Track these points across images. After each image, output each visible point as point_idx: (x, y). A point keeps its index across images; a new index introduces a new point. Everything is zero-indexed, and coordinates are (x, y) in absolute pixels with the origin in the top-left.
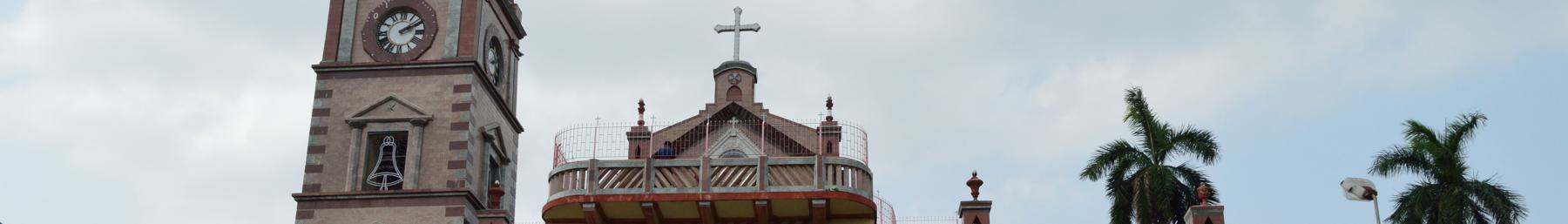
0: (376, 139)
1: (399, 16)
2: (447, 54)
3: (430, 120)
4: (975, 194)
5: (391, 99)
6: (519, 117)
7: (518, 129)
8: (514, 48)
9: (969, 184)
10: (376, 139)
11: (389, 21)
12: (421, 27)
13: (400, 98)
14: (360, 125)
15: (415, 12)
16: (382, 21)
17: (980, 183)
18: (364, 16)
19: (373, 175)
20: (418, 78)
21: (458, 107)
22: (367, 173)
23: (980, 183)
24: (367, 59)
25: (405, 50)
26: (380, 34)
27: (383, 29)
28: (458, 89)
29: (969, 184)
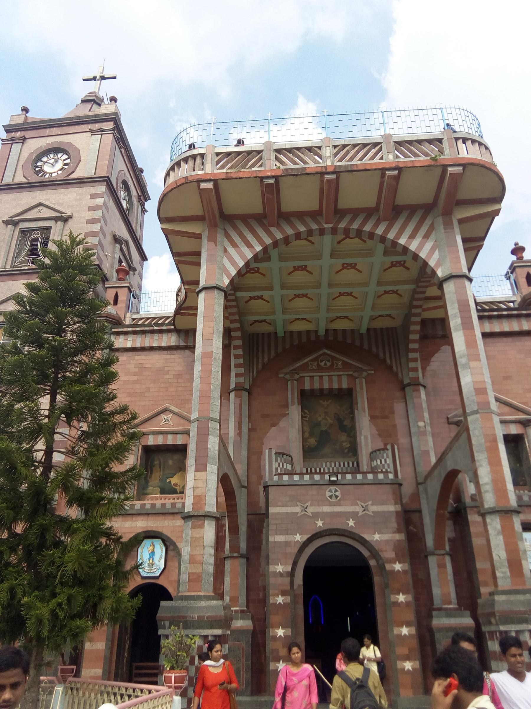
0: (24, 233)
1: (52, 156)
2: (86, 175)
3: (70, 217)
4: (520, 258)
5: (40, 204)
6: (144, 247)
7: (144, 258)
8: (143, 205)
9: (513, 252)
10: (24, 233)
11: (45, 159)
12: (68, 161)
13: (47, 203)
14: (15, 224)
15: (64, 151)
16: (39, 158)
17: (523, 249)
18: (25, 154)
19: (21, 259)
20: (63, 190)
21: (91, 209)
22: (18, 256)
23: (523, 249)
24: (24, 180)
25: (54, 175)
26: (37, 167)
27: (39, 164)
28: (93, 196)
29: (513, 252)
